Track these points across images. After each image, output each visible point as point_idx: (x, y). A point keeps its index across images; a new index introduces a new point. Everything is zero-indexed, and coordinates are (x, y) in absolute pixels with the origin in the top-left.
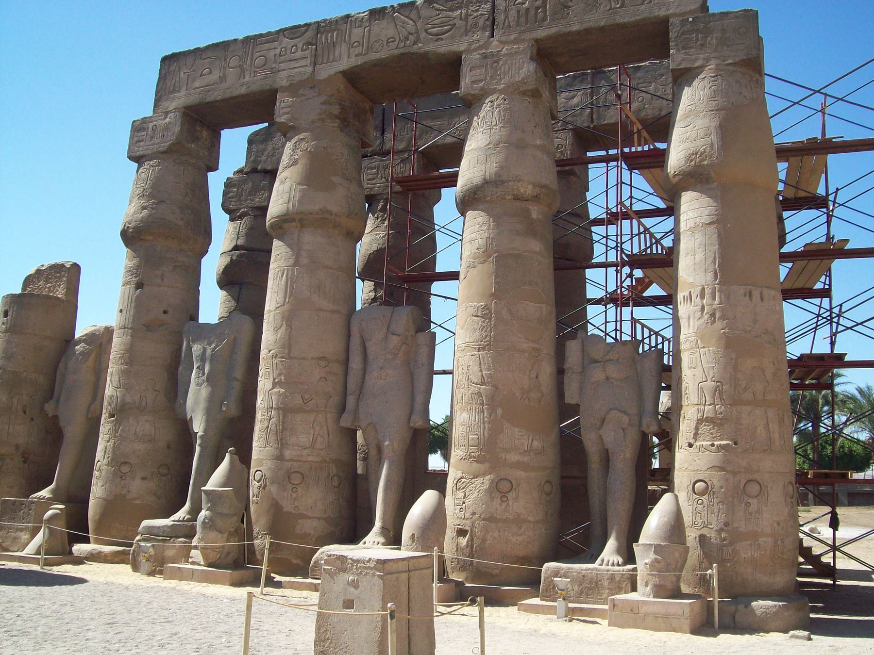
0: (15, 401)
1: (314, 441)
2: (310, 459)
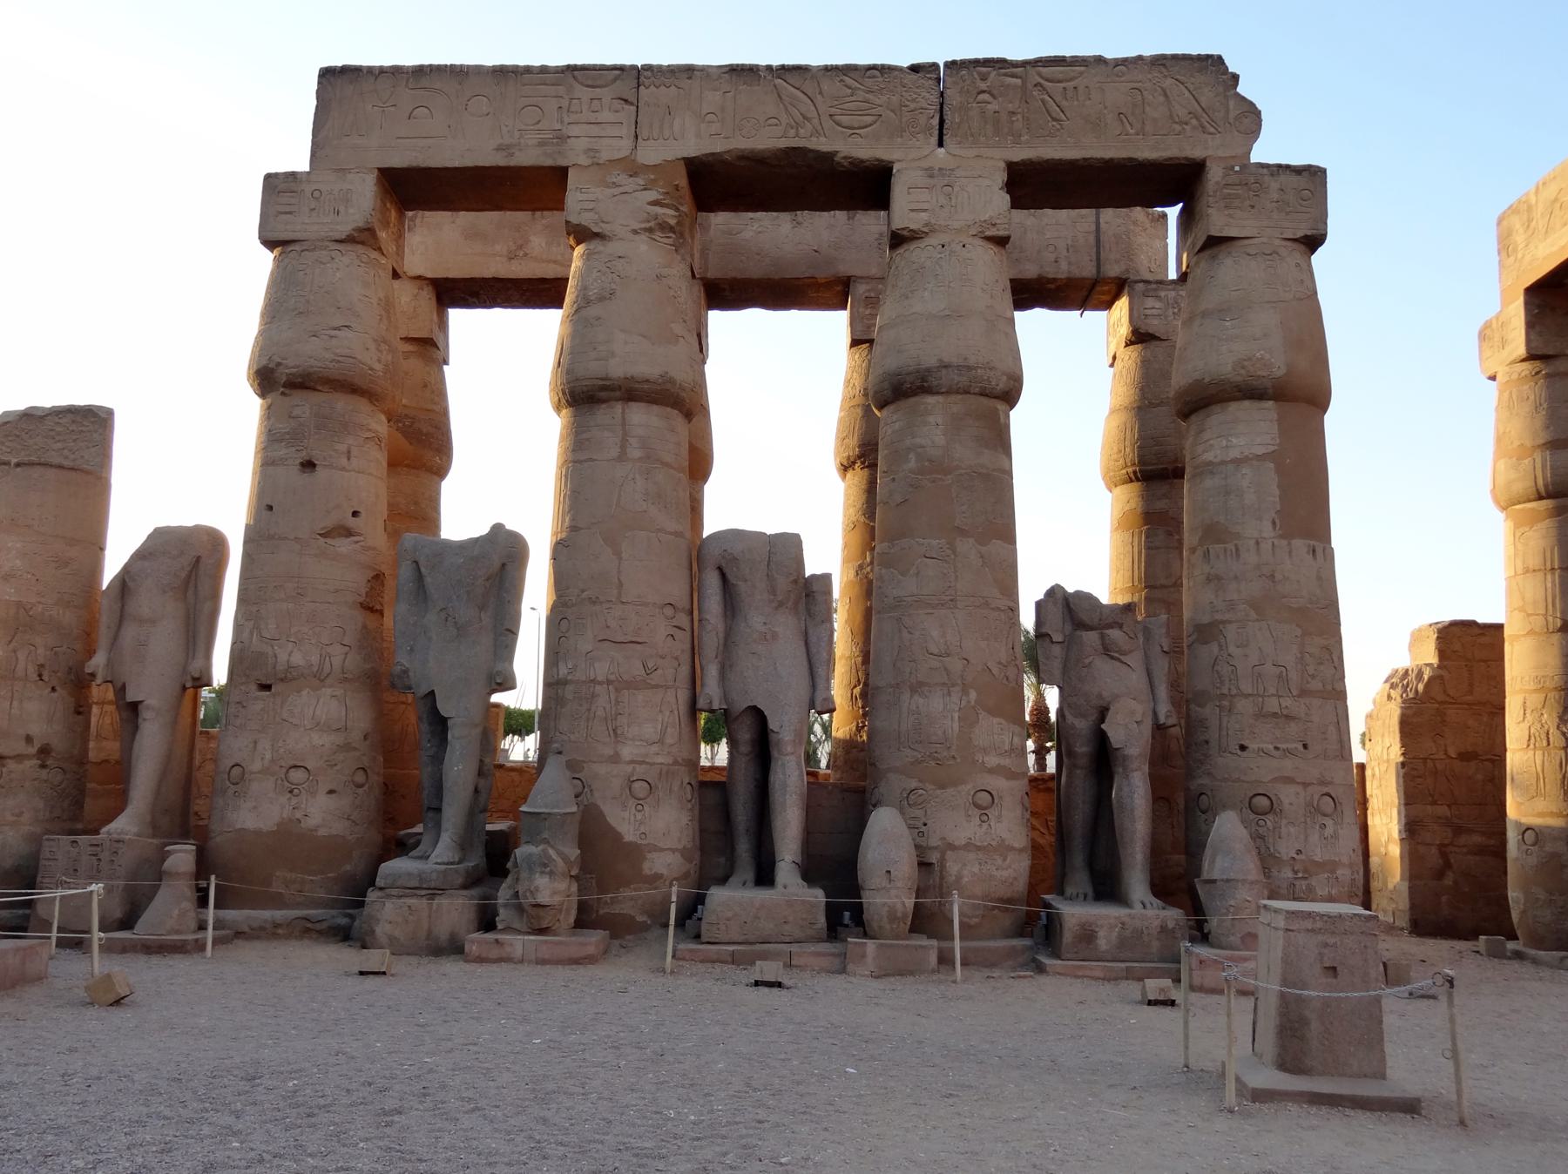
0: (22, 656)
1: (663, 733)
2: (660, 760)
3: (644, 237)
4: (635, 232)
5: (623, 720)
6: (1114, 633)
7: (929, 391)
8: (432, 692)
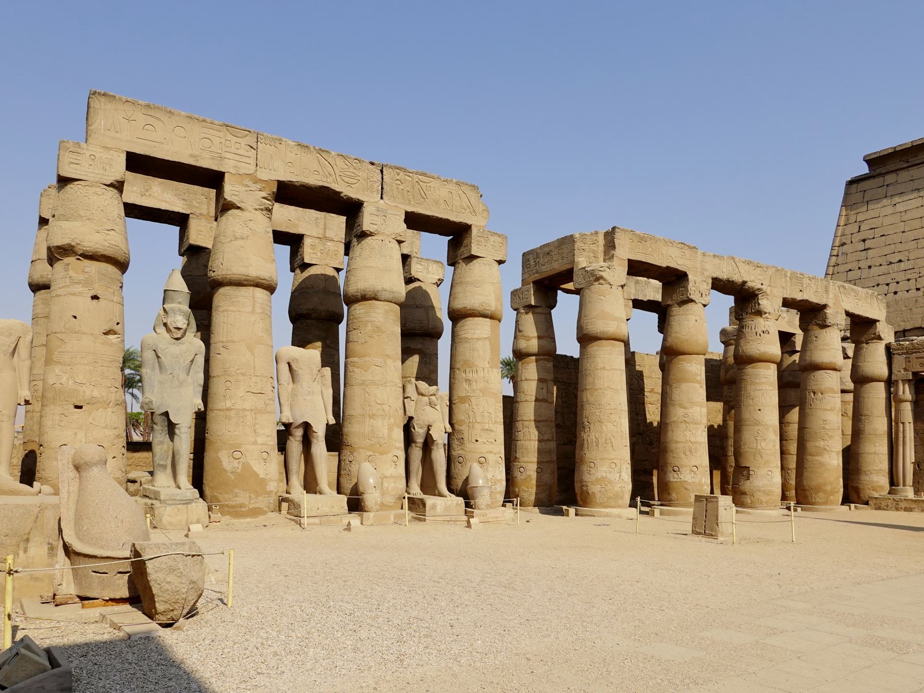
3: (259, 212)
6: (433, 398)
7: (377, 300)
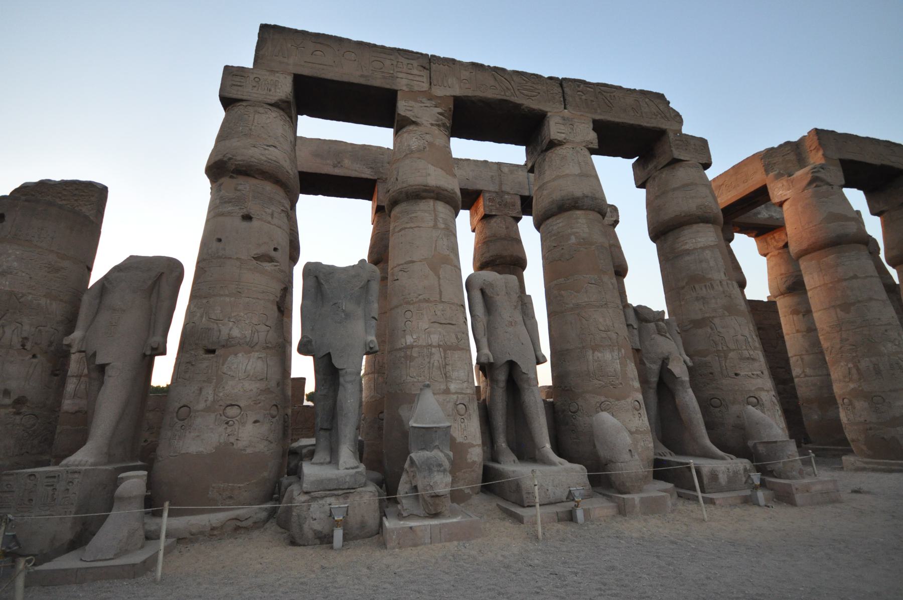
4: (432, 125)
5: (449, 368)
8: (329, 354)
